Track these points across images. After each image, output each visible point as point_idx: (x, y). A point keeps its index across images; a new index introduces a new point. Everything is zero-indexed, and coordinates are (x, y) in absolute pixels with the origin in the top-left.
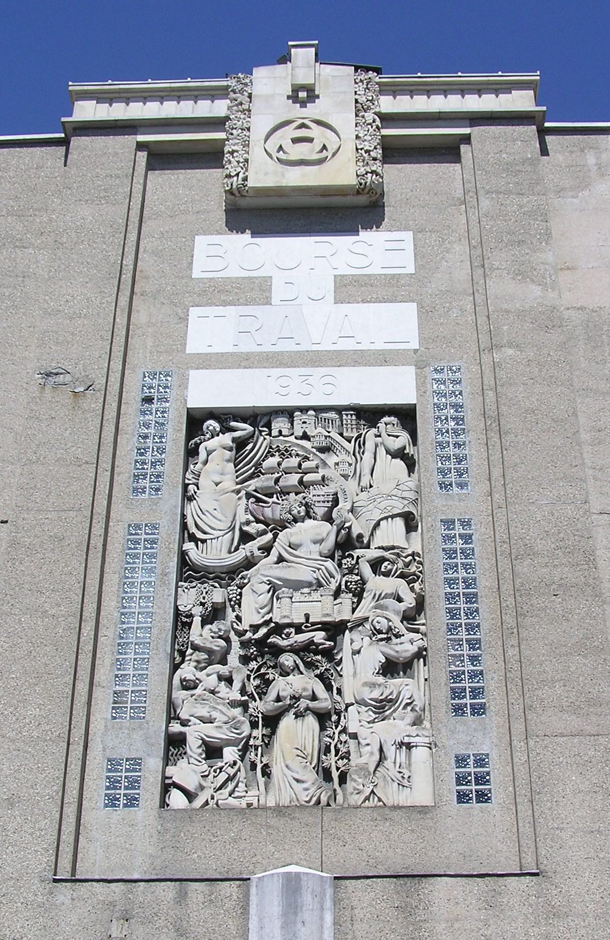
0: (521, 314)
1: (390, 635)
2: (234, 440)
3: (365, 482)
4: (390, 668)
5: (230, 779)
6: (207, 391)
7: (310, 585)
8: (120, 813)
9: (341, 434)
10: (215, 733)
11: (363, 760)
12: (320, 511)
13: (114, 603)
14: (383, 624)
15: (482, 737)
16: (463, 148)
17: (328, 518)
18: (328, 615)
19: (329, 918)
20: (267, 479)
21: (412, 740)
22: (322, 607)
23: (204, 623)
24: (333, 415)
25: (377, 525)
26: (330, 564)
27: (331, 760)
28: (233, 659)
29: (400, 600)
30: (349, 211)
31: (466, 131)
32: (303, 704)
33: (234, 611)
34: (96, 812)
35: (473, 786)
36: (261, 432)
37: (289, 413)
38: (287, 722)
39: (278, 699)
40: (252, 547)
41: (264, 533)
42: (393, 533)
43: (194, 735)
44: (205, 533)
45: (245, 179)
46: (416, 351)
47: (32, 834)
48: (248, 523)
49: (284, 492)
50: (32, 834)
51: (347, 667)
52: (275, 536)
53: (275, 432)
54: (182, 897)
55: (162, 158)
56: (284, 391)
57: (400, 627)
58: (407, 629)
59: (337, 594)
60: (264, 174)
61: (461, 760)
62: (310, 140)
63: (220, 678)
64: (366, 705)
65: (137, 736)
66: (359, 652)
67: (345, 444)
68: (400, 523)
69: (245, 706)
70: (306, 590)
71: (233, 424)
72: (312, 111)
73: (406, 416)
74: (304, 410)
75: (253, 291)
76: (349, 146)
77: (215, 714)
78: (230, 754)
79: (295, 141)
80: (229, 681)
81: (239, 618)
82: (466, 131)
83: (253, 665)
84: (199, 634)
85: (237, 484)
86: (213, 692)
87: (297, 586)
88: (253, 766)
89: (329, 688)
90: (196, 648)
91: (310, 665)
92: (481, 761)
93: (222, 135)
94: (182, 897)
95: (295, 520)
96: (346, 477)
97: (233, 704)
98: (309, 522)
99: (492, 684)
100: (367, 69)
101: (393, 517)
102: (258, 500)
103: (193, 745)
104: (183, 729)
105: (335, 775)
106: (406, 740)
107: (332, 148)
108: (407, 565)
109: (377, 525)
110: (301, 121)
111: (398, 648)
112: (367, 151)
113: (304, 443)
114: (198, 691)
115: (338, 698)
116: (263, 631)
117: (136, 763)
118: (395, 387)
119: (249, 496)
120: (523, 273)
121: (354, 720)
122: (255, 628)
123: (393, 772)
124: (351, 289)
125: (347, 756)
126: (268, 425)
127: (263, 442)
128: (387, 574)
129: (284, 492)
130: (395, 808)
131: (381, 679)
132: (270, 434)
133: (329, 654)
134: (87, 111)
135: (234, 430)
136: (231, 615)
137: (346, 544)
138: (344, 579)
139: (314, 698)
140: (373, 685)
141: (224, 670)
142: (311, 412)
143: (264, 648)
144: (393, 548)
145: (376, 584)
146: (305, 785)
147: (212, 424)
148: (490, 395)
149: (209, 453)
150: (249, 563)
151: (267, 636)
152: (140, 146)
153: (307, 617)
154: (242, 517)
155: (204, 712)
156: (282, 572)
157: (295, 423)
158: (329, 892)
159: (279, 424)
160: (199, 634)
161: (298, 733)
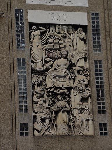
1: (83, 91)
2: (41, 32)
4: (83, 100)
5: (48, 128)
6: (33, 17)
7: (63, 77)
9: (68, 32)
10: (43, 116)
11: (77, 123)
12: (64, 56)
13: (17, 81)
14: (81, 88)
17: (66, 57)
18: (68, 86)
20: (51, 46)
21: (89, 119)
23: (38, 86)
25: (78, 60)
26: (67, 71)
27: (71, 123)
29: (84, 81)
32: (64, 109)
33: (44, 82)
36: (47, 30)
37: (55, 25)
38: (60, 114)
39: (58, 108)
40: (47, 65)
41: (50, 61)
42: (81, 63)
43: (39, 116)
44: (36, 60)
46: (87, 7)
47: (7, 144)
48: (46, 58)
49: (56, 50)
50: (7, 144)
52: (53, 62)
53: (51, 31)
56: (53, 19)
57: (84, 89)
58: (86, 89)
63: (43, 101)
64: (78, 109)
65: (27, 117)
66: (76, 96)
67: (69, 36)
68: (83, 60)
70: (62, 78)
71: (40, 27)
73: (84, 28)
74: (59, 25)
77: (43, 111)
78: (47, 121)
80: (45, 102)
81: (46, 85)
83: (51, 98)
84: (37, 89)
85: (42, 45)
89: (69, 104)
90: (36, 93)
91: (65, 98)
95: (59, 58)
96: (70, 46)
97: (47, 108)
98: (62, 59)
101: (82, 58)
104: (36, 115)
105: (72, 127)
106: (88, 119)
108: (86, 72)
109: (78, 60)
111: (84, 94)
113: (59, 35)
114: (38, 104)
115: (71, 107)
116: (53, 89)
118: (82, 19)
119: (46, 50)
121: (76, 113)
122: (51, 88)
123: (85, 127)
126: (49, 28)
128: (81, 74)
129: (56, 50)
130: (86, 136)
131: (81, 103)
132: (49, 31)
136: (44, 84)
137: (71, 65)
138: (71, 75)
140: (80, 105)
142: (61, 26)
143: (53, 94)
144: (82, 67)
145: (79, 77)
146: (66, 130)
149: (34, 36)
150: (47, 69)
153: (63, 85)
155: (41, 110)
156: (55, 73)
157: (57, 29)
159: (52, 28)
160: (37, 89)
161: (62, 116)
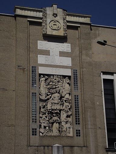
0: (87, 62)
2: (45, 79)
3: (64, 88)
4: (68, 116)
5: (48, 131)
6: (42, 70)
7: (57, 103)
8: (34, 136)
11: (64, 129)
12: (58, 92)
15: (79, 127)
16: (79, 28)
17: (59, 93)
19: (62, 151)
22: (58, 107)
24: (59, 76)
26: (59, 100)
27: (60, 129)
28: (47, 113)
29: (69, 106)
30: (61, 39)
31: (79, 25)
32: (57, 121)
34: (31, 136)
35: (78, 133)
37: (53, 75)
38: (55, 124)
39: (53, 120)
41: (50, 95)
42: (67, 96)
43: (43, 125)
45: (46, 32)
48: (48, 93)
49: (53, 88)
51: (62, 116)
52: (52, 95)
54: (44, 148)
55: (32, 23)
59: (61, 105)
60: (49, 32)
61: (77, 130)
62: (56, 25)
63: (45, 117)
68: (68, 94)
69: (48, 121)
72: (57, 19)
73: (69, 77)
74: (55, 75)
75: (46, 53)
76: (62, 28)
77: (45, 122)
78: (47, 128)
79: (54, 25)
80: (46, 117)
81: (47, 108)
82: (79, 25)
83: (50, 115)
84: (42, 110)
86: (45, 119)
87: (55, 103)
88: (50, 130)
89: (60, 119)
91: (57, 115)
92: (79, 131)
93: (41, 21)
94: (44, 148)
96: (61, 87)
97: (47, 121)
98: (57, 94)
99: (81, 120)
100: (65, 10)
102: (49, 89)
103: (42, 127)
107: (60, 27)
108: (69, 101)
110: (55, 21)
112: (65, 29)
114: (43, 118)
116: (51, 110)
117: (36, 129)
118: (68, 72)
119: (48, 88)
120: (87, 55)
121: (63, 124)
122: (50, 110)
123: (68, 132)
124: (62, 54)
125: (62, 129)
126: (50, 77)
127: (49, 80)
129: (53, 88)
130: (69, 136)
131: (66, 118)
133: (60, 114)
134: (19, 12)
135: (46, 77)
136: (46, 107)
137: (61, 97)
139: (58, 120)
140: (66, 119)
141: (46, 115)
143: (51, 113)
145: (66, 104)
147: (42, 76)
148: (82, 76)
150: (48, 99)
151: (51, 111)
152: (28, 21)
153: (57, 108)
154: (47, 92)
155: (44, 122)
156: (53, 101)
158: (62, 148)
159: (52, 77)
160: (42, 110)
161: (56, 125)
